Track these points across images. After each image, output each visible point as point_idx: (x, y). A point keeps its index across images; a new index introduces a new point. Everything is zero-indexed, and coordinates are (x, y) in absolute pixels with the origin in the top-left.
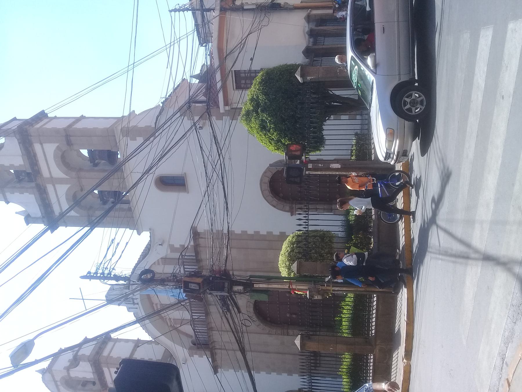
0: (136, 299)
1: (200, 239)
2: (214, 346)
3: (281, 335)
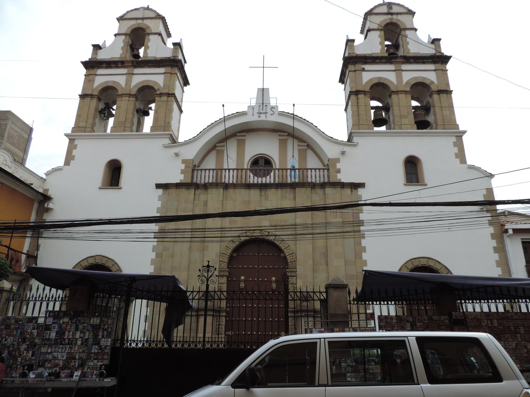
0: (266, 117)
1: (350, 189)
2: (198, 189)
3: (219, 268)
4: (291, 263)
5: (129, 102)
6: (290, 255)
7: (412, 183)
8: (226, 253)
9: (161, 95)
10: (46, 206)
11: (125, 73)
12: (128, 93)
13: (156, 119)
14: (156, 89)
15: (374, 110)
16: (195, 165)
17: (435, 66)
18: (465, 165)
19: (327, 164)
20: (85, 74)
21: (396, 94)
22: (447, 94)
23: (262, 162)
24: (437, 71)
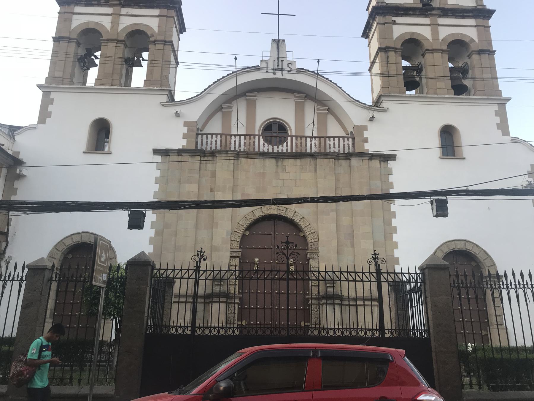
2: (205, 156)
3: (231, 248)
4: (312, 243)
5: (117, 49)
6: (311, 235)
7: (447, 156)
8: (238, 232)
9: (155, 42)
10: (18, 172)
11: (110, 13)
12: (115, 37)
13: (150, 72)
14: (150, 36)
15: (405, 71)
16: (198, 128)
17: (476, 21)
18: (509, 137)
19: (351, 132)
20: (59, 11)
21: (431, 53)
22: (489, 54)
23: (275, 128)
24: (478, 27)
